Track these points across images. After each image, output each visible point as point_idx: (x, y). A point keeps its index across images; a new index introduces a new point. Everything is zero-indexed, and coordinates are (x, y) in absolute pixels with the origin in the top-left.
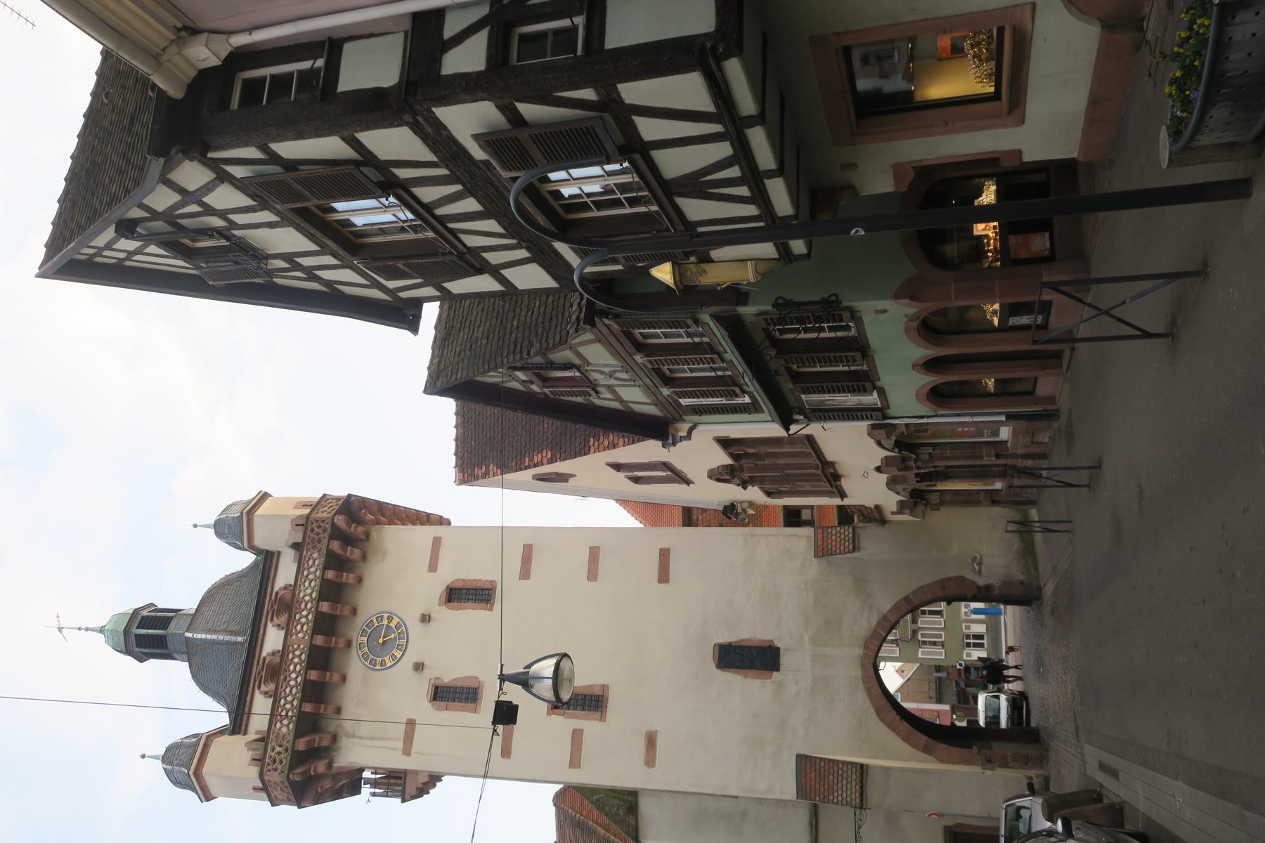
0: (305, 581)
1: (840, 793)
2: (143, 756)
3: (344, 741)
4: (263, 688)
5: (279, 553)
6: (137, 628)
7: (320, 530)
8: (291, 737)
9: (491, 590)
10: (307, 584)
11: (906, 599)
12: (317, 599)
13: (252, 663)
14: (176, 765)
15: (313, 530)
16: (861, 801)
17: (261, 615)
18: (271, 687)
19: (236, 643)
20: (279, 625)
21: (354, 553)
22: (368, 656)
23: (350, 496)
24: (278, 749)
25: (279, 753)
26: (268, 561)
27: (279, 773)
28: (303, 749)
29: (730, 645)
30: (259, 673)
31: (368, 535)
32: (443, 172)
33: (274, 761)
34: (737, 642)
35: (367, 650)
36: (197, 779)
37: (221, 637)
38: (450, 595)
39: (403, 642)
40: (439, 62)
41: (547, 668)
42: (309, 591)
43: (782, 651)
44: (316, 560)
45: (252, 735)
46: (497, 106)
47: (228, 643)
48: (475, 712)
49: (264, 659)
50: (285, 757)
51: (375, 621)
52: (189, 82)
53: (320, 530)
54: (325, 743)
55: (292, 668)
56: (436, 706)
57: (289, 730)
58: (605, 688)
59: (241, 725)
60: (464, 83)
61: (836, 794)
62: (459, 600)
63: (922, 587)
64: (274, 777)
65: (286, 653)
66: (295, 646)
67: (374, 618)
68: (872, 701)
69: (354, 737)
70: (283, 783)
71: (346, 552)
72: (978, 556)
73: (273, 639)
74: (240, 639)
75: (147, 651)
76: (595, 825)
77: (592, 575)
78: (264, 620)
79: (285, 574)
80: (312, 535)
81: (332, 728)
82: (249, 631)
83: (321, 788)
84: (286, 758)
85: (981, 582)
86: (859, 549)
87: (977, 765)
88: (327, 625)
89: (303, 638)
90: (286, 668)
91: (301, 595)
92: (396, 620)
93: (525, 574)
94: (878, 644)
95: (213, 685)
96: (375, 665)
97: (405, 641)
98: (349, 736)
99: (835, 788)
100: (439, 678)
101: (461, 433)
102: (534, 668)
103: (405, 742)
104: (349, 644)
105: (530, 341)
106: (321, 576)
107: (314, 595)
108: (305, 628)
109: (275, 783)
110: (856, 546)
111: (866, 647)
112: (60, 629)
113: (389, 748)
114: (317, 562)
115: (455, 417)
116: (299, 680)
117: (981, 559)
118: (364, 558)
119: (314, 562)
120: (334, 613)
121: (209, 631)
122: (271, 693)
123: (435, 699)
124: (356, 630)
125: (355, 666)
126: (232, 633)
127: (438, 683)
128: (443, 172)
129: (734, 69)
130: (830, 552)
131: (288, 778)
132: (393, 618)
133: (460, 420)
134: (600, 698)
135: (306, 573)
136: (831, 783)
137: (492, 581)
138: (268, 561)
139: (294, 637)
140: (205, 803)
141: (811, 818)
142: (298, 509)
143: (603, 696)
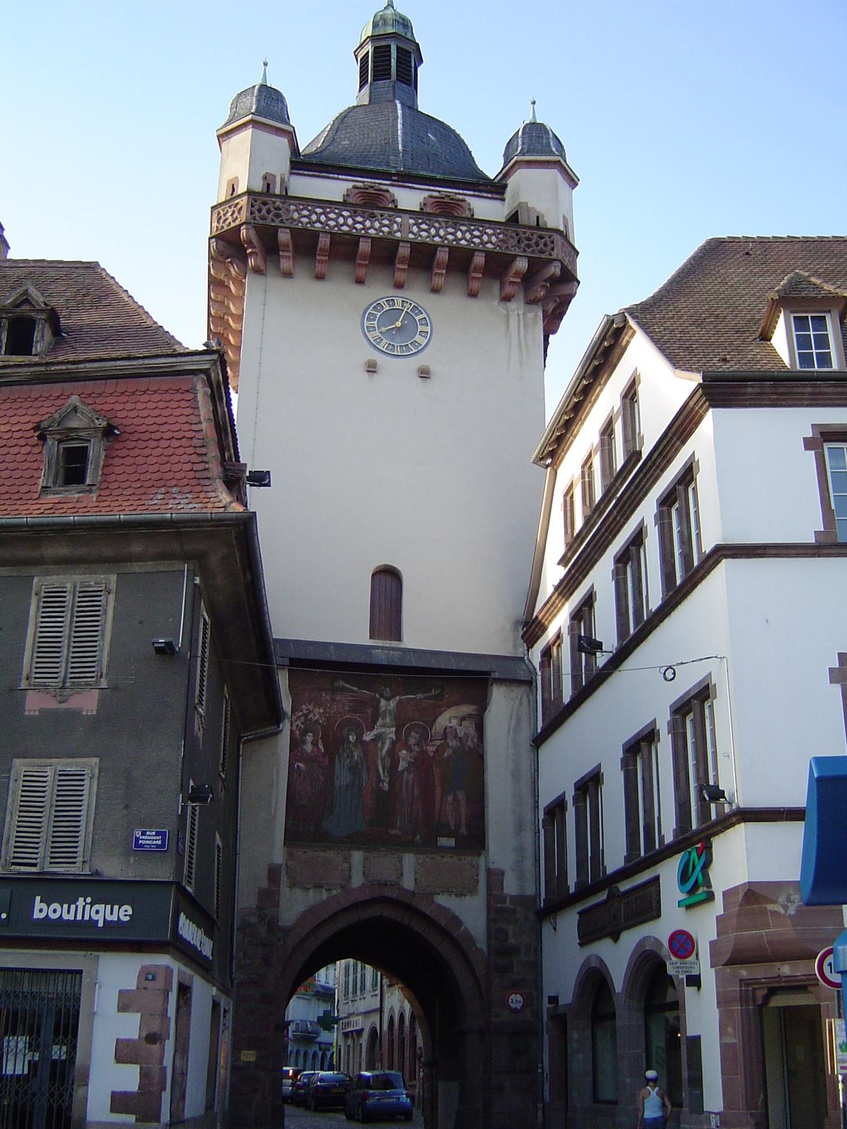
12: (459, 246)
26: (496, 188)
35: (386, 309)
73: (409, 198)
79: (483, 208)
88: (423, 257)
89: (412, 232)
90: (358, 213)
124: (417, 296)
125: (378, 292)
138: (496, 188)
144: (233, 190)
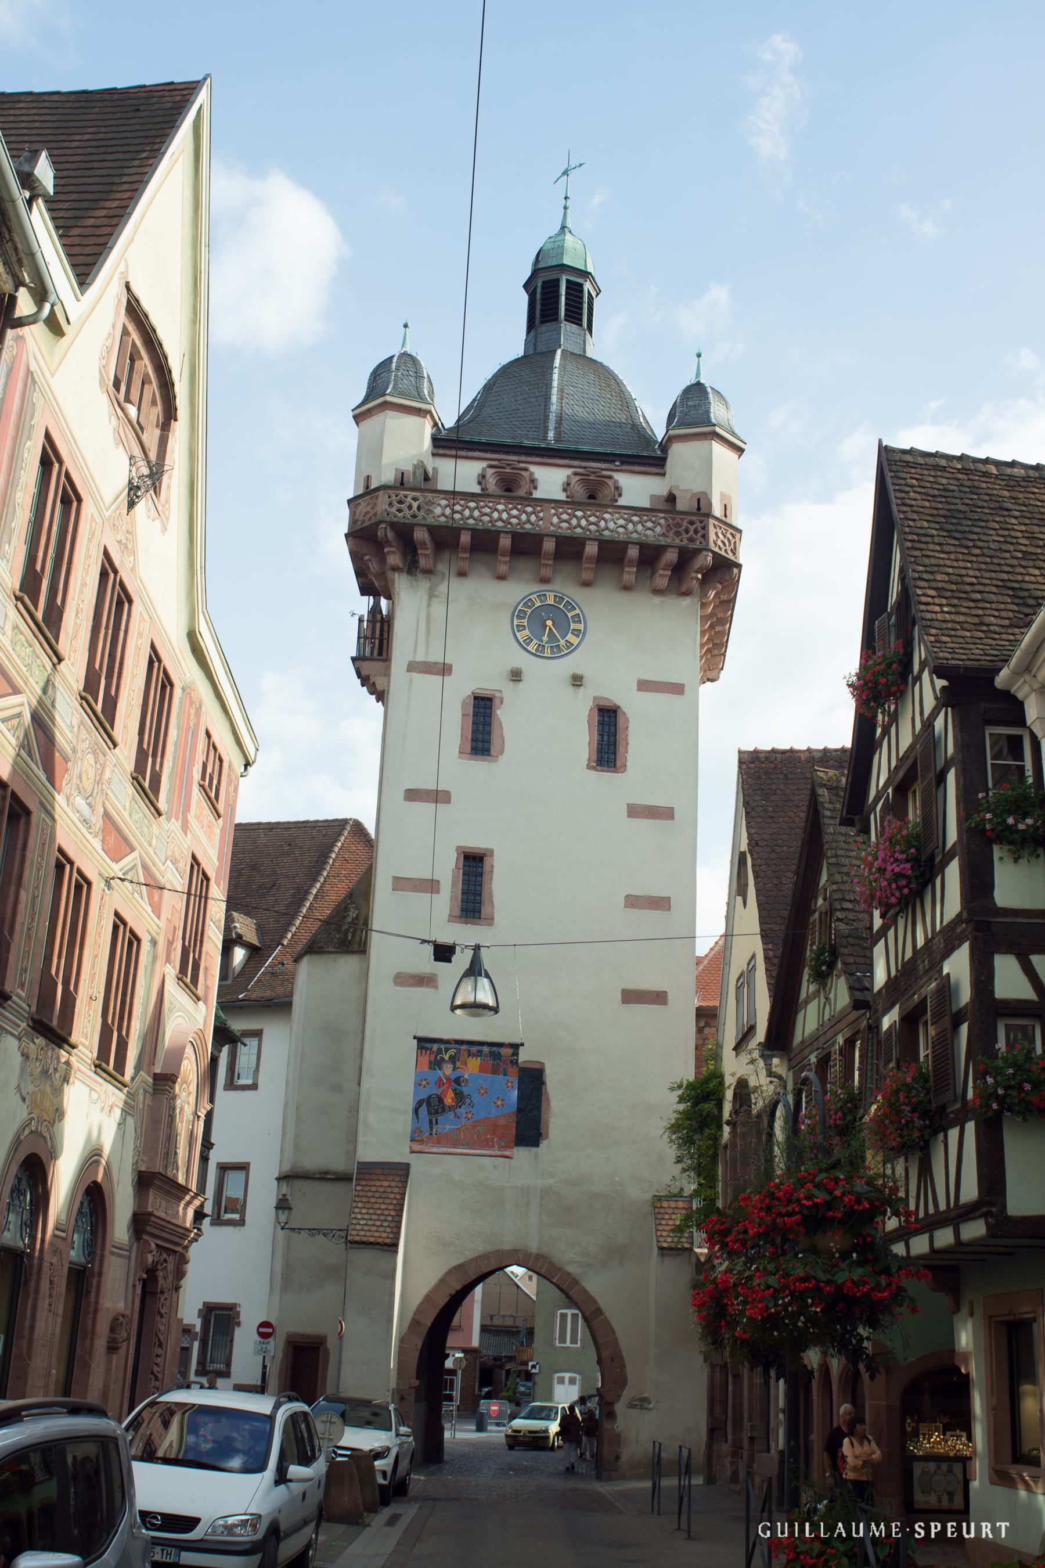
0: (625, 519)
1: (366, 1216)
2: (406, 326)
3: (424, 584)
4: (490, 471)
5: (664, 475)
6: (568, 281)
7: (692, 533)
8: (430, 520)
9: (615, 766)
10: (621, 522)
11: (599, 1311)
12: (600, 538)
13: (520, 454)
14: (396, 376)
15: (692, 523)
16: (356, 1242)
17: (583, 459)
18: (491, 482)
19: (546, 429)
20: (568, 484)
21: (663, 576)
22: (530, 608)
23: (739, 566)
24: (415, 505)
25: (410, 507)
27: (386, 510)
28: (415, 538)
29: (542, 1083)
30: (509, 465)
31: (687, 594)
32: (938, 928)
33: (400, 502)
34: (546, 1092)
36: (379, 405)
38: (608, 711)
39: (548, 653)
40: (1008, 951)
41: (485, 996)
42: (611, 525)
43: (534, 1149)
44: (652, 531)
45: (430, 464)
46: (967, 1004)
47: (546, 418)
48: (460, 752)
49: (526, 469)
50: (404, 516)
51: (574, 613)
52: (1012, 692)
53: (692, 533)
54: (422, 562)
55: (515, 512)
56: (468, 701)
57: (438, 517)
58: (490, 921)
59: (444, 447)
60: (983, 978)
61: (364, 1211)
62: (601, 723)
63: (614, 1333)
64: (382, 503)
65: (532, 504)
66: (541, 514)
67: (578, 611)
68: (472, 1260)
69: (430, 599)
70: (375, 515)
71: (663, 569)
72: (651, 1406)
74: (551, 434)
75: (538, 296)
76: (322, 879)
77: (633, 902)
78: (576, 463)
80: (685, 523)
81: (441, 567)
82: (560, 446)
83: (370, 560)
84: (404, 517)
85: (619, 1408)
86: (662, 1255)
87: (398, 1384)
89: (552, 524)
91: (607, 516)
92: (575, 640)
93: (635, 811)
94: (543, 1272)
95: (494, 399)
96: (518, 617)
97: (549, 655)
98: (431, 596)
99: (371, 1211)
100: (502, 702)
101: (800, 757)
102: (486, 981)
103: (425, 663)
104: (545, 581)
105: (854, 920)
106: (631, 540)
107: (606, 533)
108: (565, 525)
109: (375, 504)
110: (666, 1252)
111: (539, 1256)
113: (416, 643)
114: (649, 532)
115: (821, 747)
116: (500, 524)
117: (647, 1409)
118: (657, 592)
119: (649, 529)
120: (584, 560)
121: (561, 390)
122: (483, 483)
123: (476, 698)
127: (496, 702)
128: (938, 928)
129: (975, 1230)
130: (660, 1216)
131: (382, 522)
132: (578, 636)
133: (817, 755)
134: (477, 915)
135: (635, 519)
136: (377, 1206)
137: (625, 766)
139: (553, 511)
140: (351, 414)
141: (334, 1173)
142: (722, 500)
143: (480, 918)
144: (367, 487)
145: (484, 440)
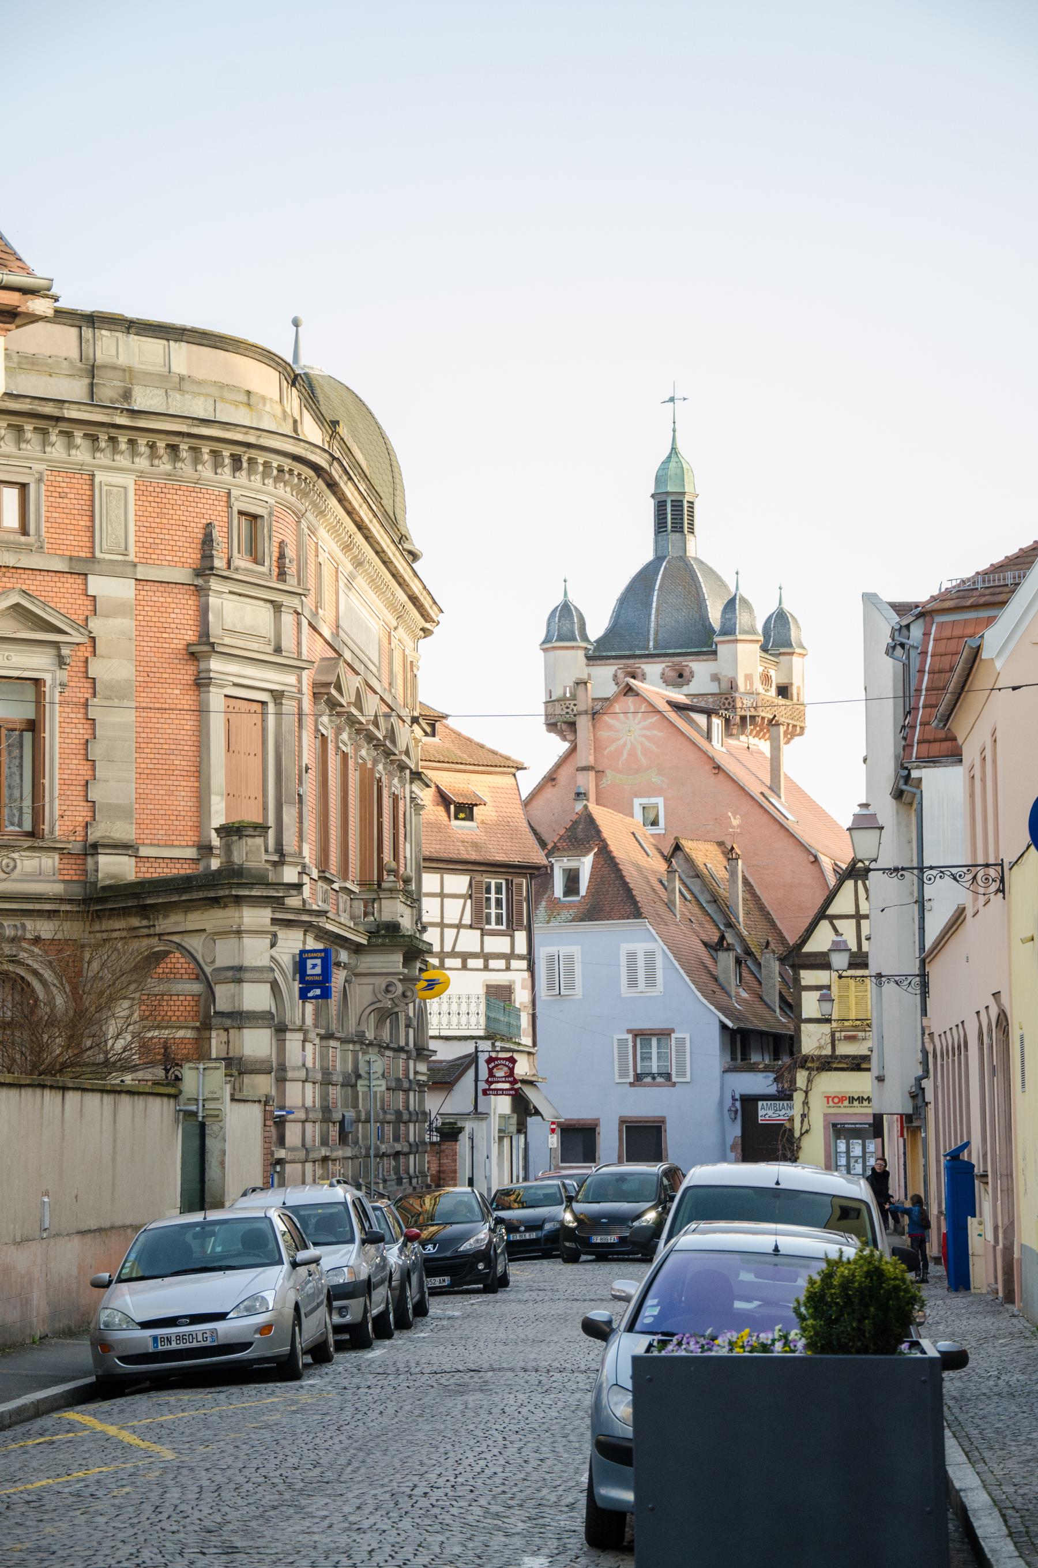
4: (620, 671)
37: (653, 625)
74: (651, 644)
112: (672, 400)
121: (657, 609)
126: (656, 634)
145: (613, 654)
